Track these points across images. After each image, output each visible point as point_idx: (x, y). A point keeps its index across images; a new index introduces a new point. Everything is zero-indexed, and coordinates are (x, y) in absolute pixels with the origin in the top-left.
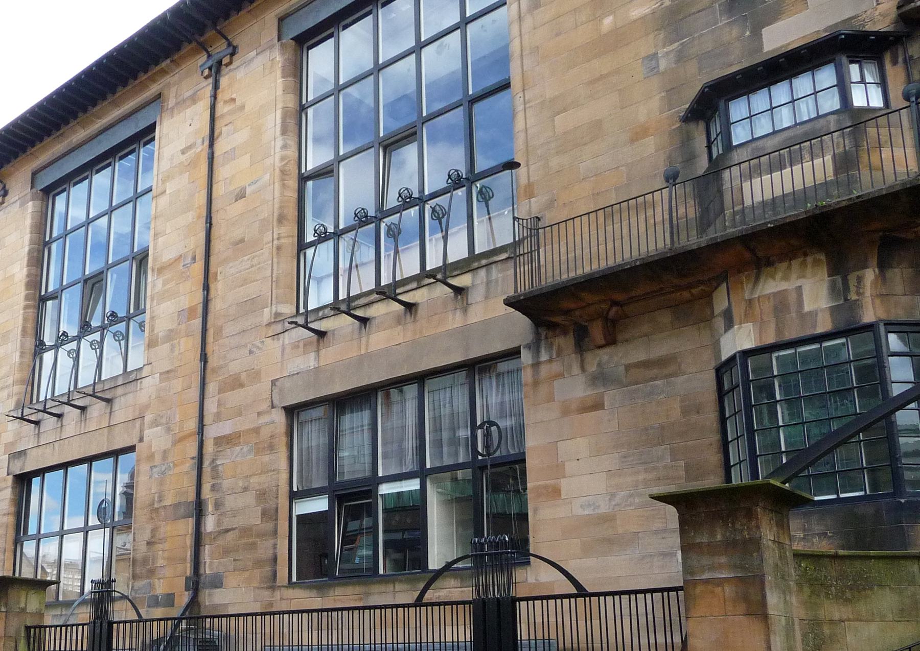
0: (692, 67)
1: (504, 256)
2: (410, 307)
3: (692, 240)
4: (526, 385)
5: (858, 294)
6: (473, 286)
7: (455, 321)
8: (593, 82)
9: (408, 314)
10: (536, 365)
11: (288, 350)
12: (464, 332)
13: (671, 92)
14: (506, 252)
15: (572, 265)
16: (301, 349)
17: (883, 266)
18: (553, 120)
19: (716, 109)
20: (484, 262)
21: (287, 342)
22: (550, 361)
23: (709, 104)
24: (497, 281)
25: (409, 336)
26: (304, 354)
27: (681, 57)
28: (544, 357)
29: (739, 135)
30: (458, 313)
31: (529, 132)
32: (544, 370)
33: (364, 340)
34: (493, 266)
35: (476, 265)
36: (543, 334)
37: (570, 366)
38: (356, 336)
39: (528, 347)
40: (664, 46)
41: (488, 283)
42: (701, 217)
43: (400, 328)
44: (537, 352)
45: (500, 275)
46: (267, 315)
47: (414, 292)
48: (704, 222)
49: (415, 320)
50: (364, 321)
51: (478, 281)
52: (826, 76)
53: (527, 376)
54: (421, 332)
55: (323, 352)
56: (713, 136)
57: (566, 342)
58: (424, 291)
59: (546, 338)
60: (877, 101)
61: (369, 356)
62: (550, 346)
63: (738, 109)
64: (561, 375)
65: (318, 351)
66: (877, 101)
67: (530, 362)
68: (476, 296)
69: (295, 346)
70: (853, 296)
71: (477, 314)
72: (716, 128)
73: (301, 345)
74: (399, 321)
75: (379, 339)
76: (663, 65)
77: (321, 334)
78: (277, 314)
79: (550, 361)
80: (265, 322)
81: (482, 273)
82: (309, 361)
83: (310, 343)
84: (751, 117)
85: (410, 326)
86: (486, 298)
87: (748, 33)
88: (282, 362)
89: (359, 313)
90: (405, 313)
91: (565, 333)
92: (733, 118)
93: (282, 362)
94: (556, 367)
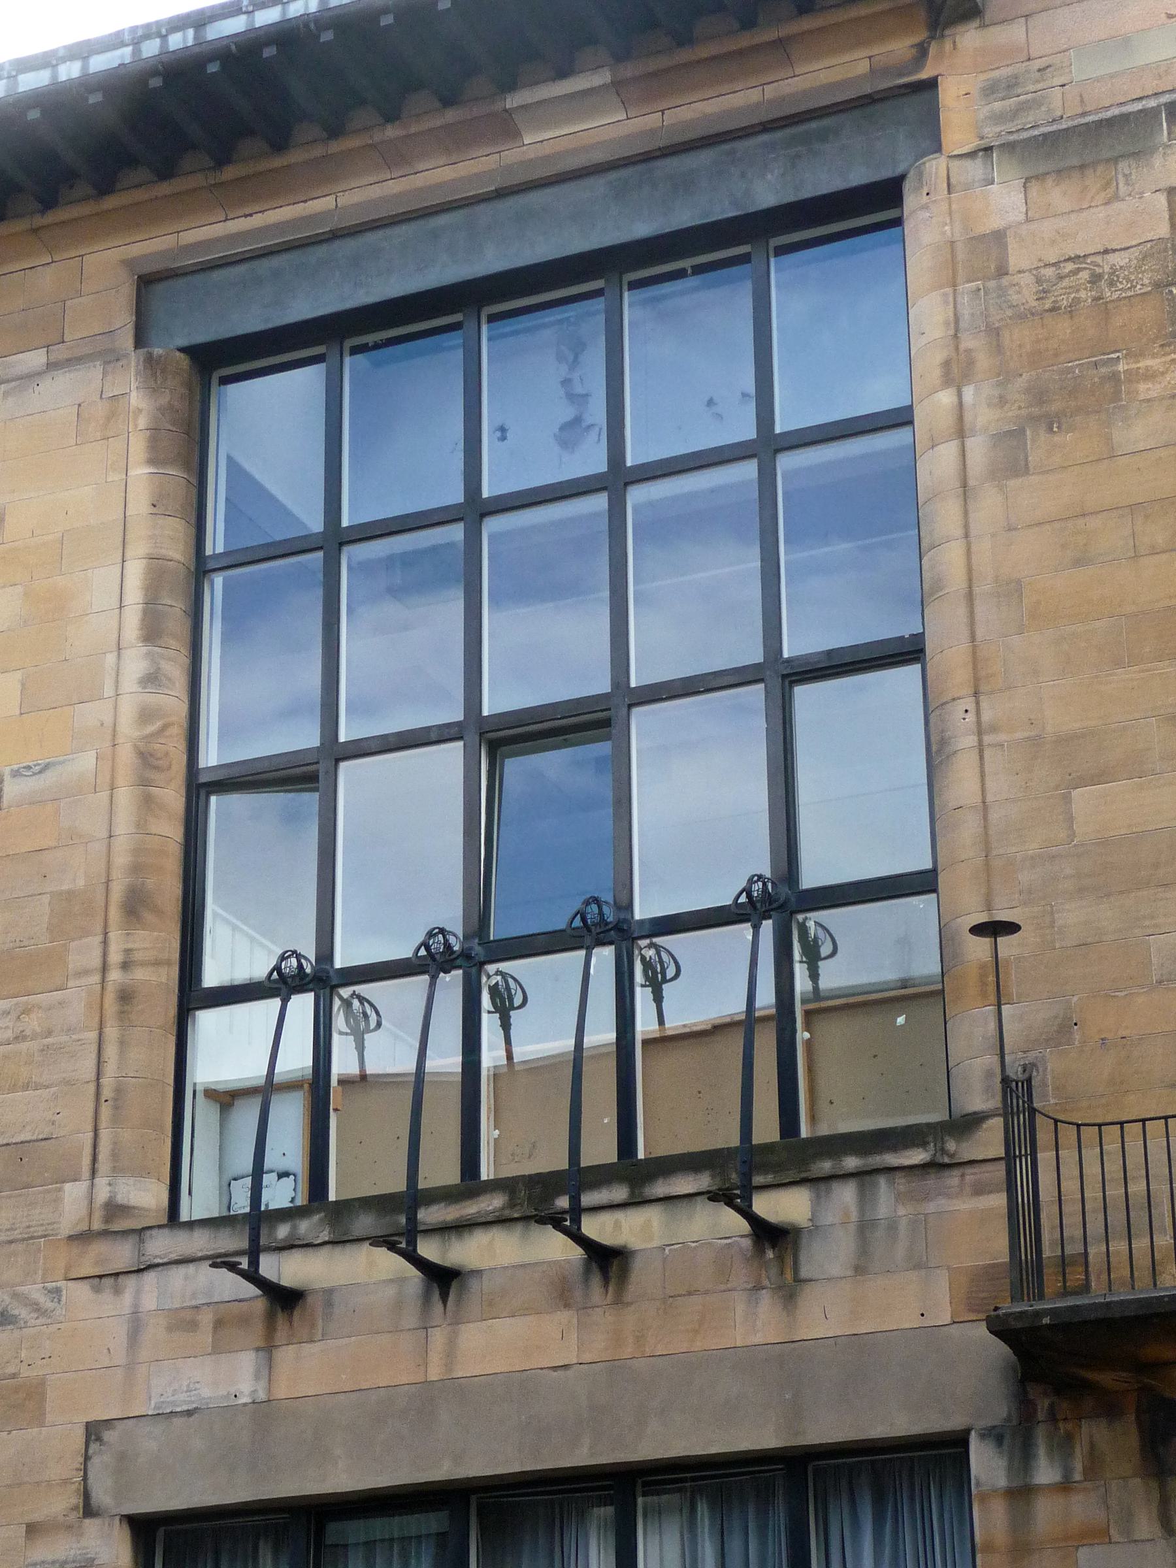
1: (917, 1156)
2: (606, 1261)
4: (989, 1548)
6: (816, 1228)
7: (754, 1323)
9: (596, 1280)
10: (1021, 1494)
11: (154, 1331)
12: (787, 1364)
14: (924, 1145)
15: (1139, 1218)
16: (206, 1336)
18: (1067, 799)
20: (851, 1163)
21: (149, 1302)
22: (1065, 1486)
24: (892, 1226)
25: (598, 1348)
26: (217, 1349)
28: (1045, 1473)
30: (766, 1300)
31: (994, 816)
32: (1046, 1513)
33: (438, 1337)
34: (882, 1181)
35: (826, 1166)
36: (1043, 1405)
37: (1127, 1519)
38: (410, 1319)
39: (995, 1435)
41: (865, 1227)
43: (565, 1317)
44: (1023, 1458)
45: (901, 1211)
46: (73, 1203)
47: (619, 1215)
49: (618, 1301)
50: (442, 1280)
51: (829, 1217)
53: (990, 1520)
54: (639, 1339)
55: (286, 1355)
57: (1114, 1440)
58: (651, 1216)
59: (1053, 1418)
61: (457, 1390)
62: (1063, 1447)
64: (1097, 1535)
65: (268, 1348)
67: (1002, 1482)
68: (827, 1258)
69: (183, 1321)
71: (825, 1316)
73: (206, 1319)
74: (562, 1294)
75: (489, 1344)
77: (285, 1299)
78: (114, 1209)
79: (1065, 1486)
80: (66, 1227)
81: (846, 1194)
82: (236, 1378)
83: (243, 1321)
85: (603, 1318)
86: (860, 1270)
88: (130, 1367)
89: (428, 1249)
90: (587, 1271)
91: (1110, 1409)
93: (130, 1367)
94: (1082, 1507)
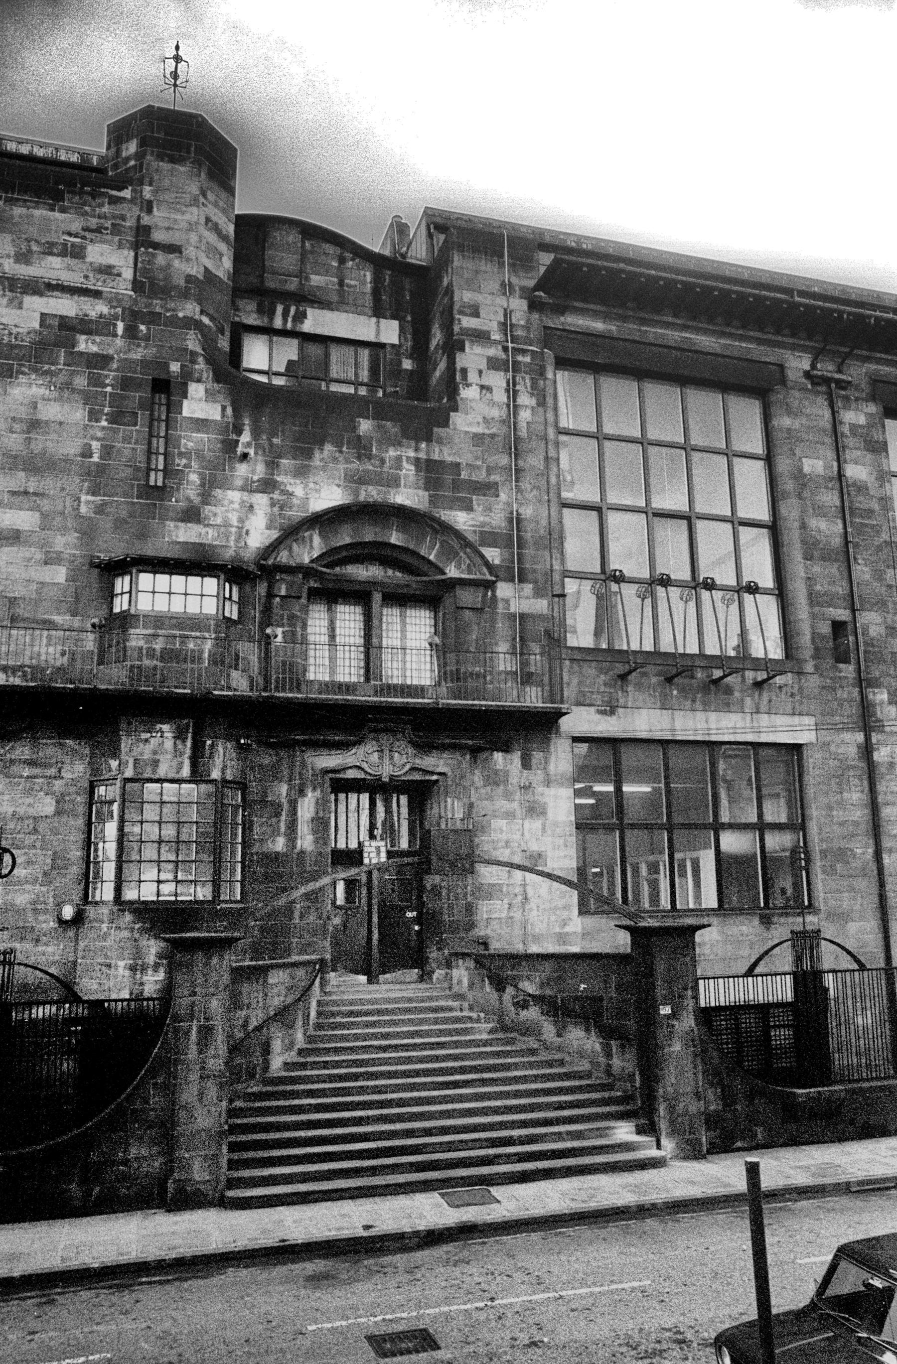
8: (14, 493)
27: (100, 509)
40: (88, 493)
52: (211, 584)
60: (235, 617)
63: (145, 580)
76: (83, 509)
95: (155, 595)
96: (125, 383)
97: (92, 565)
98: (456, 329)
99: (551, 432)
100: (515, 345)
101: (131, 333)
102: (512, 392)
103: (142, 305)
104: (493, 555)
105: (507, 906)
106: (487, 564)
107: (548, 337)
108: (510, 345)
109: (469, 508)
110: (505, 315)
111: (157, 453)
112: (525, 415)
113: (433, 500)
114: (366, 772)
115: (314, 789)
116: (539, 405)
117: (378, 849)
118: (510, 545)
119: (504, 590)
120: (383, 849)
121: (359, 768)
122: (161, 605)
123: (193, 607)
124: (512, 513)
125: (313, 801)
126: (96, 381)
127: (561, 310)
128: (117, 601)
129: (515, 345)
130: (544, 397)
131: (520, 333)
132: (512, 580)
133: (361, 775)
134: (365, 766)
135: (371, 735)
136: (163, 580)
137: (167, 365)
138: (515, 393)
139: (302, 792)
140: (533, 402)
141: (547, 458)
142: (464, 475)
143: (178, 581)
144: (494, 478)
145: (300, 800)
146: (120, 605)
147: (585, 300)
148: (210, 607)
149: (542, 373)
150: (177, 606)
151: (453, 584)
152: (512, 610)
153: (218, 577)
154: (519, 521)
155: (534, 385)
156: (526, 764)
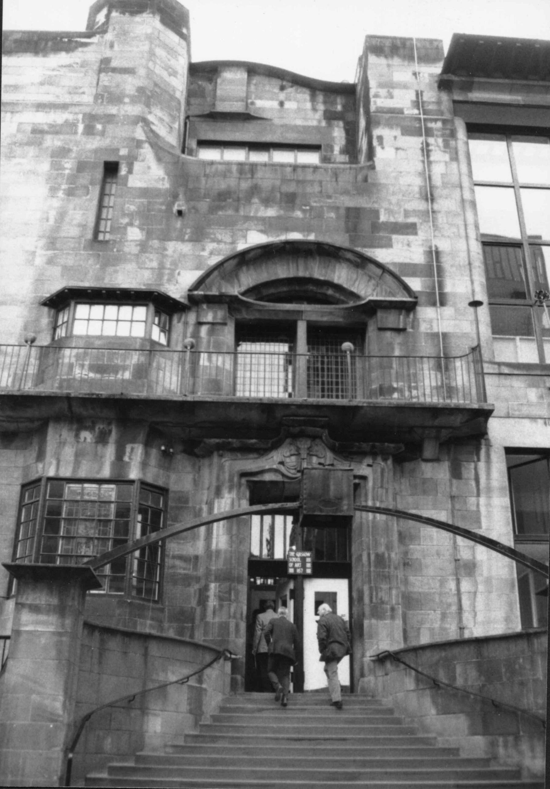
0: (56, 271)
3: (29, 388)
5: (130, 459)
13: (39, 281)
17: (147, 445)
19: (68, 305)
23: (61, 302)
29: (79, 329)
42: (38, 375)
48: (40, 378)
52: (141, 312)
56: (60, 322)
63: (82, 310)
66: (163, 340)
70: (126, 459)
72: (63, 317)
84: (89, 320)
87: (98, 266)
92: (77, 316)
95: (89, 322)
96: (81, 167)
97: (44, 304)
98: (373, 108)
99: (466, 183)
100: (425, 116)
101: (89, 131)
102: (426, 151)
103: (100, 110)
104: (416, 284)
105: (439, 616)
106: (406, 288)
107: (458, 106)
108: (422, 116)
109: (389, 245)
110: (417, 94)
111: (107, 219)
112: (438, 170)
113: (352, 240)
114: (283, 475)
115: (230, 491)
116: (452, 159)
117: (303, 559)
118: (431, 275)
119: (426, 313)
120: (309, 560)
121: (276, 471)
122: (95, 329)
123: (123, 331)
124: (431, 247)
125: (229, 501)
126: (56, 166)
127: (468, 87)
128: (58, 331)
129: (425, 116)
130: (457, 153)
131: (431, 107)
132: (434, 304)
133: (279, 478)
134: (282, 469)
135: (288, 441)
136: (97, 310)
137: (118, 150)
138: (428, 151)
139: (218, 493)
140: (447, 157)
141: (463, 201)
142: (383, 218)
143: (111, 310)
144: (411, 220)
145: (216, 501)
146: (61, 332)
147: (488, 76)
148: (139, 331)
149: (453, 134)
150: (110, 330)
151: (373, 308)
152: (435, 330)
153: (146, 305)
154: (437, 253)
155: (446, 145)
156: (456, 473)
